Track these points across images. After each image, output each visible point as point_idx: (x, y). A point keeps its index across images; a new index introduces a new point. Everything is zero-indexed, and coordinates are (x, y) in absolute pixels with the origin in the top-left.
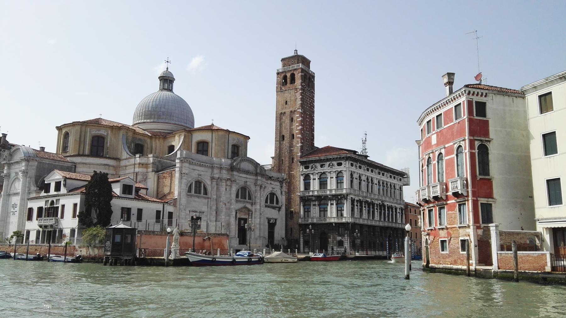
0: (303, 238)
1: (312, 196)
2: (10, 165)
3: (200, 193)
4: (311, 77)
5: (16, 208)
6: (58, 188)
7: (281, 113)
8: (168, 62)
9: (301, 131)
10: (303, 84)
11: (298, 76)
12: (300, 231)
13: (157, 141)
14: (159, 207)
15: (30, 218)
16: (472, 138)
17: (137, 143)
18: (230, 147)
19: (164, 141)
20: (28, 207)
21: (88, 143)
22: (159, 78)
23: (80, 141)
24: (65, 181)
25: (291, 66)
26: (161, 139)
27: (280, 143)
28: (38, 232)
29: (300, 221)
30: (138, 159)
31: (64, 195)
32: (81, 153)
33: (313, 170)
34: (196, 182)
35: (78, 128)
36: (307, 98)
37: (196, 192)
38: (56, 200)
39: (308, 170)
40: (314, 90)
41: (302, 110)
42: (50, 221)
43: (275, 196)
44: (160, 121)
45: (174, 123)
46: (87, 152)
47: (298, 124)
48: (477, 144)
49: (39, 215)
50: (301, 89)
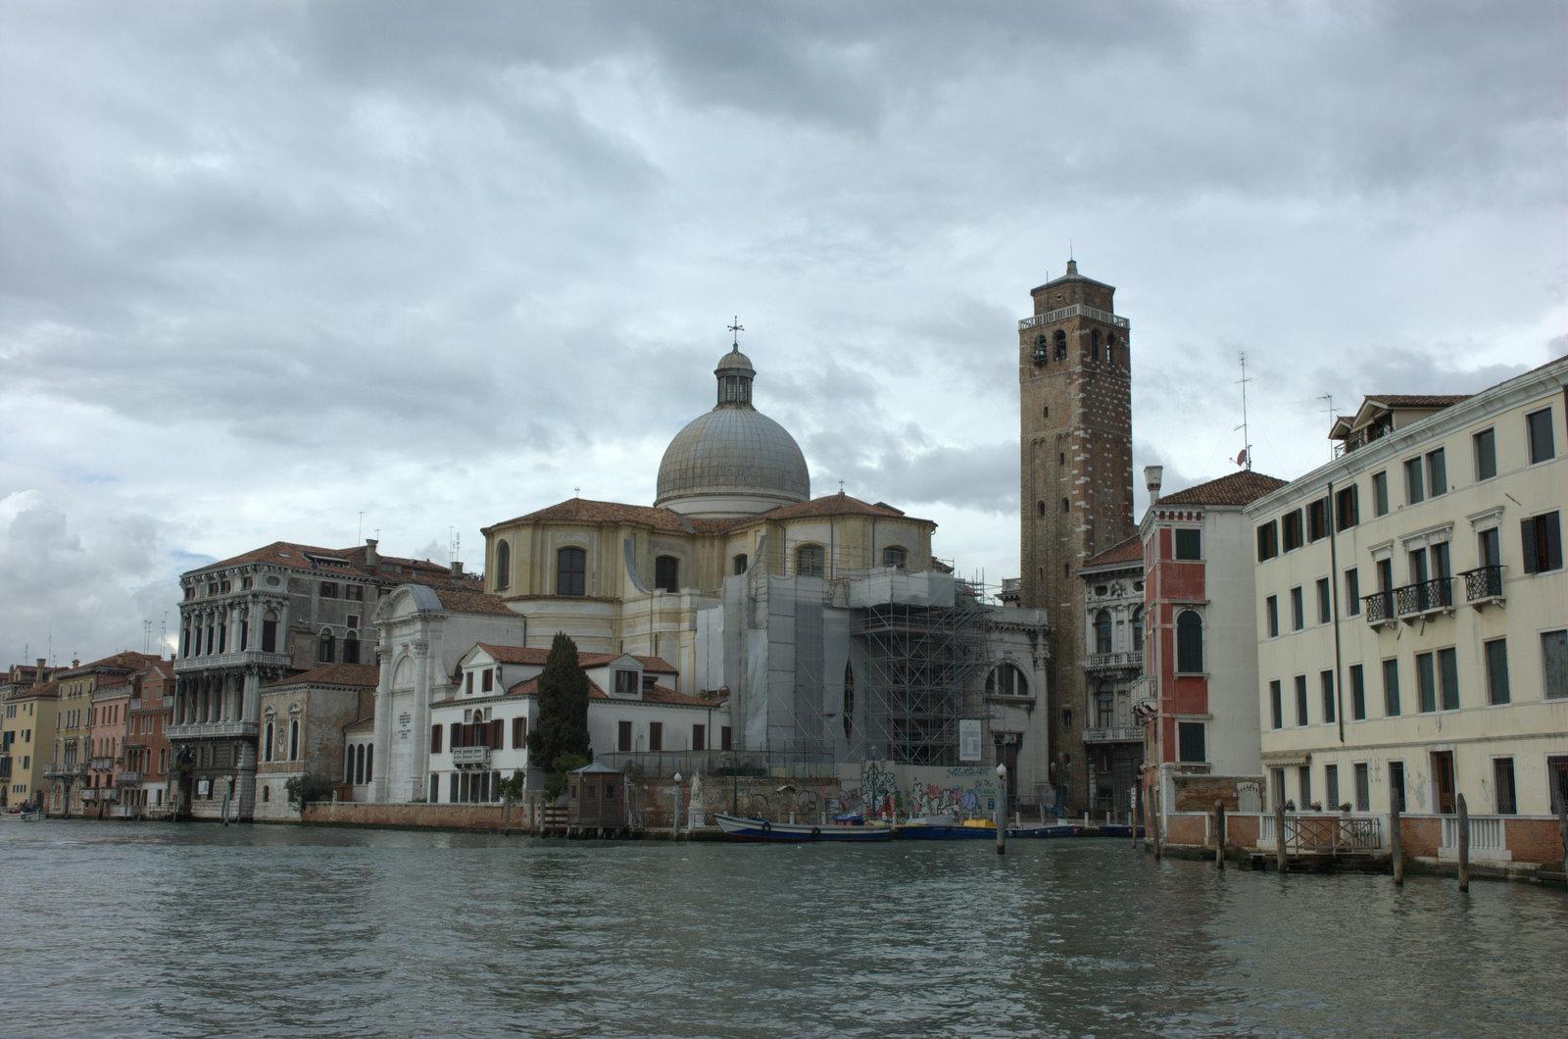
0: (1097, 783)
1: (1116, 669)
2: (389, 627)
4: (1116, 334)
7: (1035, 442)
8: (736, 328)
9: (1086, 491)
10: (1088, 359)
11: (1074, 337)
12: (1088, 764)
13: (707, 544)
14: (700, 717)
15: (436, 747)
16: (1166, 601)
17: (661, 553)
19: (725, 544)
20: (433, 724)
21: (548, 565)
22: (716, 372)
23: (532, 565)
24: (499, 668)
25: (1054, 312)
26: (716, 543)
27: (1033, 523)
28: (454, 777)
29: (1086, 737)
30: (662, 601)
31: (497, 699)
32: (537, 592)
33: (1115, 597)
35: (526, 533)
36: (1107, 395)
38: (485, 709)
39: (1104, 597)
40: (1128, 369)
41: (1086, 433)
42: (476, 754)
43: (1016, 674)
44: (713, 490)
45: (752, 492)
46: (549, 588)
47: (1076, 472)
48: (1176, 612)
49: (455, 743)
50: (1083, 375)
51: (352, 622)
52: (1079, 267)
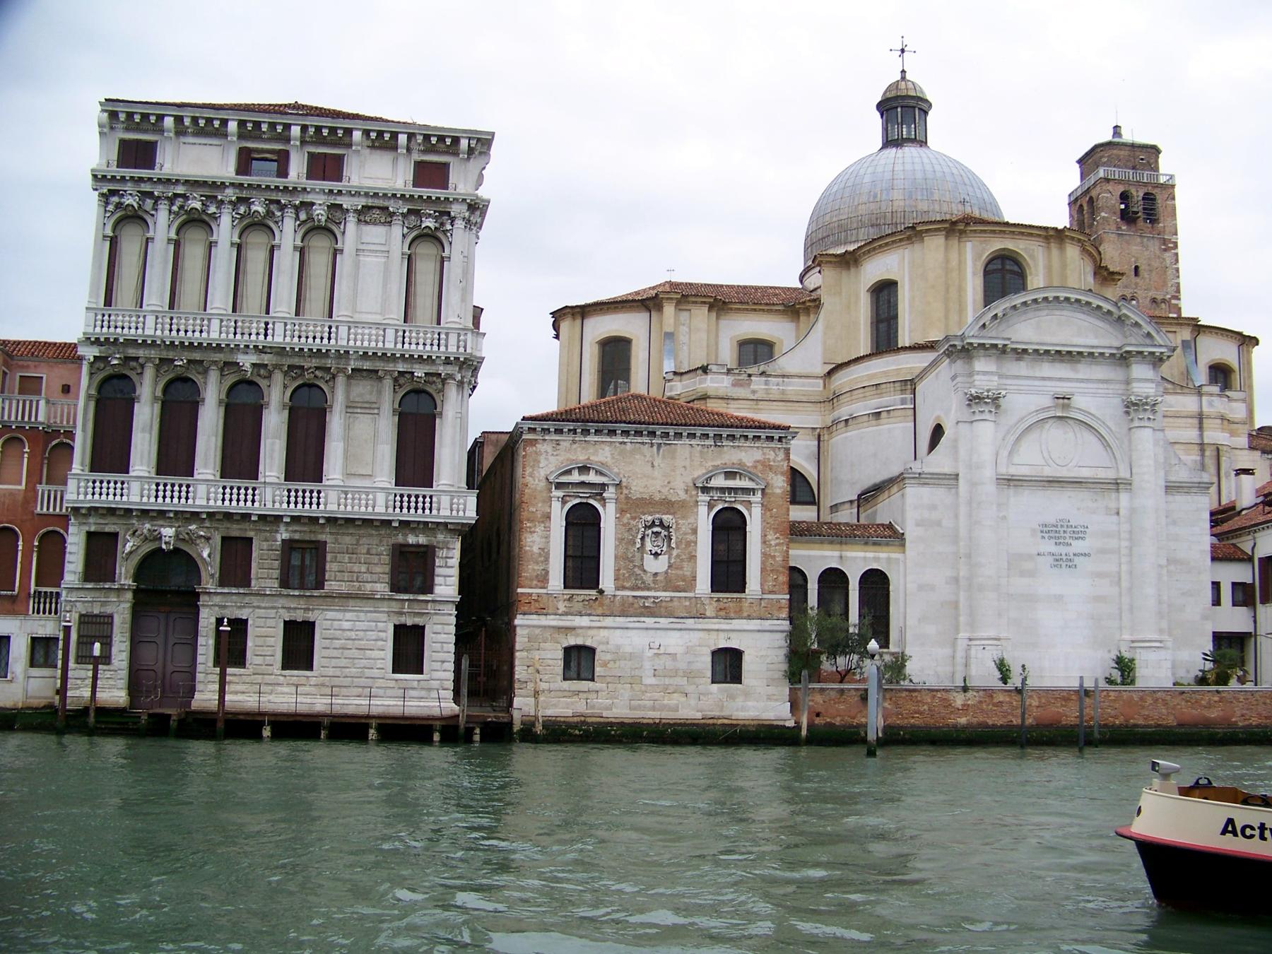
5: (1074, 543)
8: (903, 51)
52: (1123, 132)
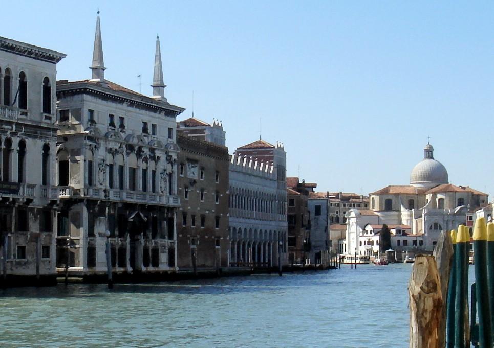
2: (349, 219)
3: (437, 229)
6: (371, 233)
15: (361, 245)
18: (457, 200)
34: (434, 224)
37: (434, 229)
42: (369, 247)
46: (384, 209)
49: (365, 244)
51: (337, 212)
